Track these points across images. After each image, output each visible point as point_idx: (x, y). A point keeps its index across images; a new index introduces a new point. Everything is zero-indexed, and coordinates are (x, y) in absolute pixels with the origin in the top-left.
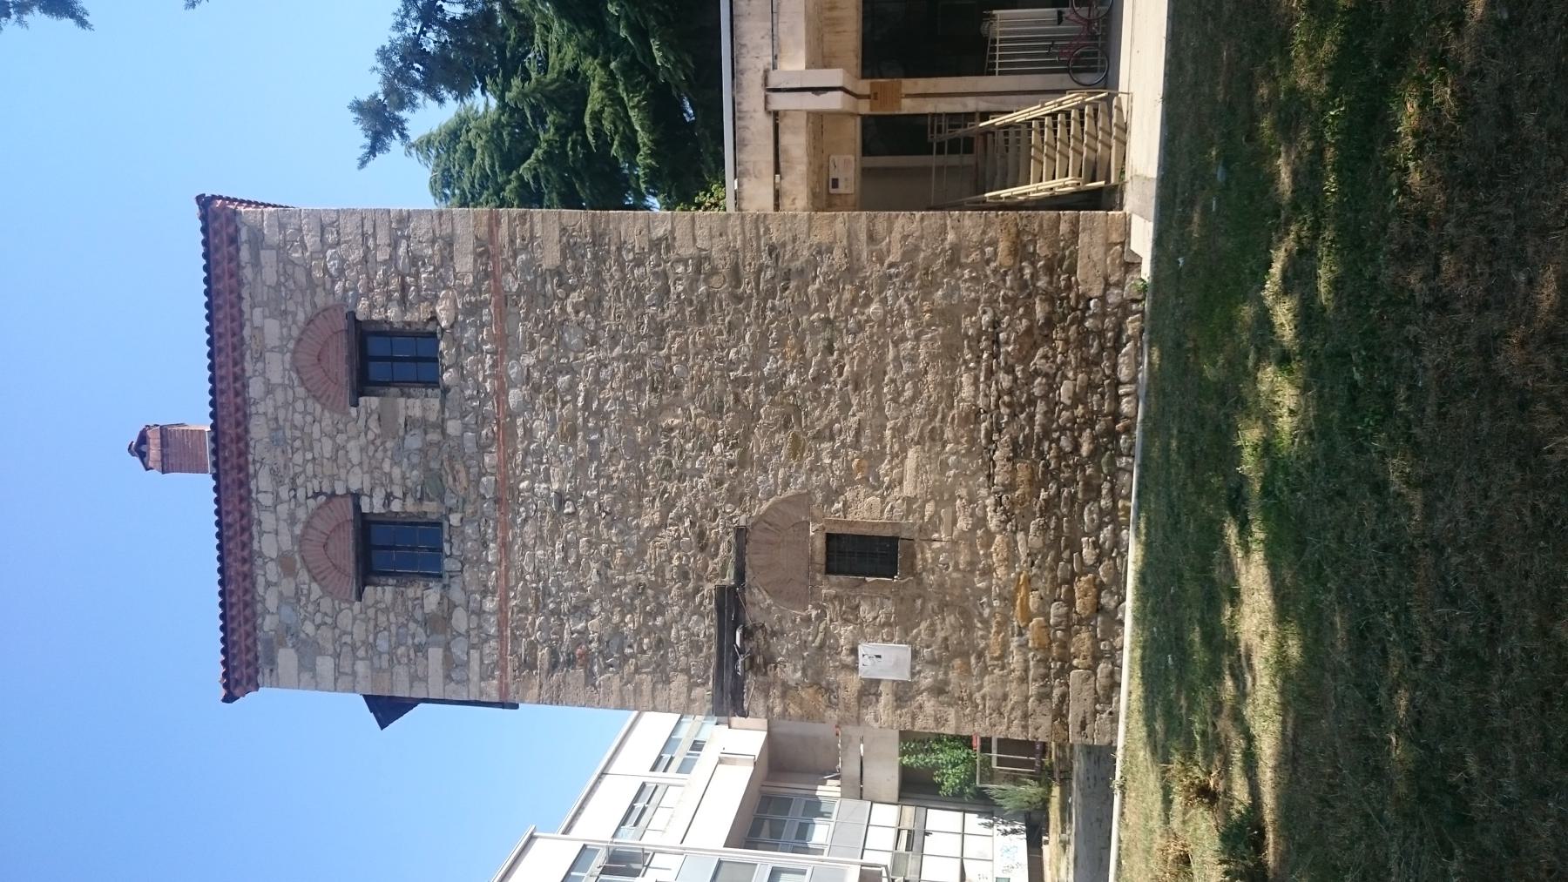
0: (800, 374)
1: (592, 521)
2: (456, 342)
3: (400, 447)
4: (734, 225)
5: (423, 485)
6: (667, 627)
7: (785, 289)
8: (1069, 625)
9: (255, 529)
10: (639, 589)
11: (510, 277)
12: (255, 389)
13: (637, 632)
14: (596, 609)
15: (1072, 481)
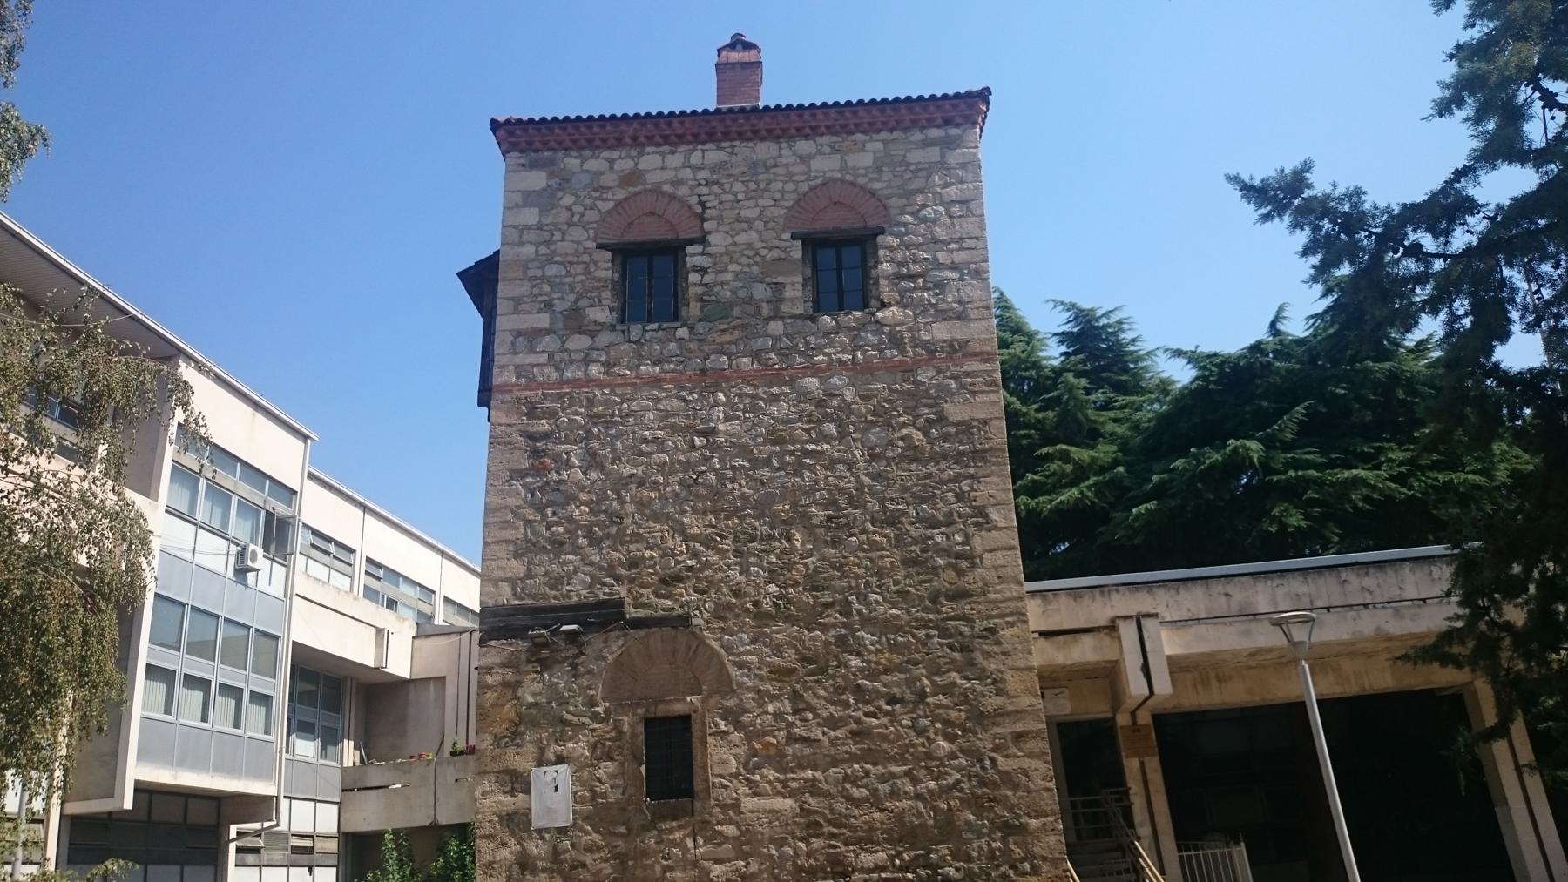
0: (861, 670)
1: (687, 466)
2: (862, 326)
3: (754, 280)
4: (1014, 590)
5: (717, 302)
7: (952, 648)
11: (931, 373)
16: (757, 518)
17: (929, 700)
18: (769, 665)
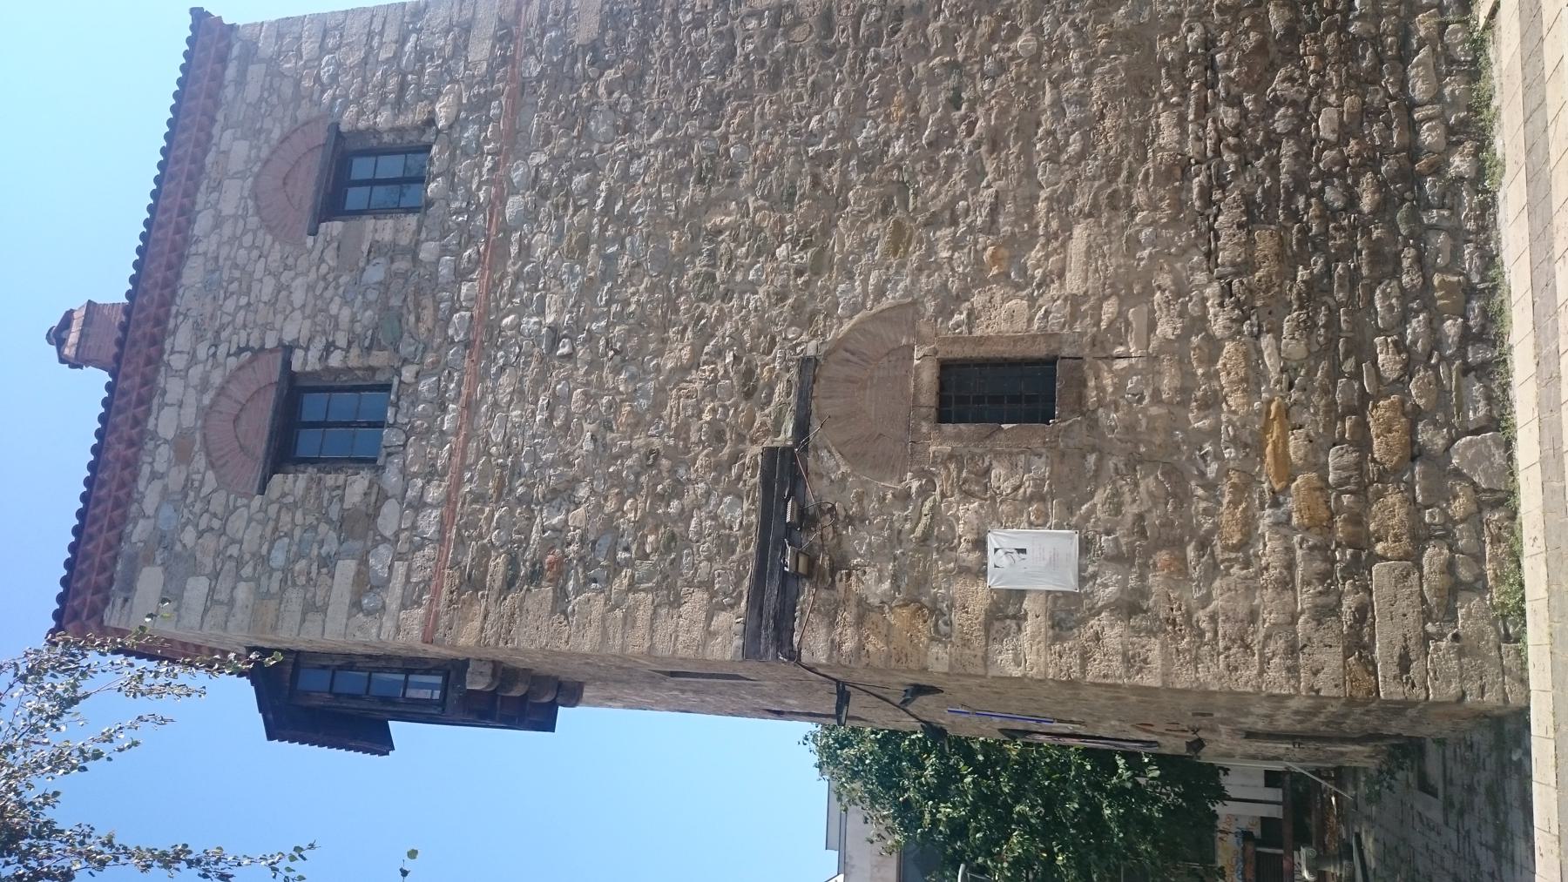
0: (909, 140)
1: (594, 364)
2: (453, 145)
5: (376, 329)
6: (684, 516)
7: (894, 32)
8: (1363, 484)
9: (155, 401)
10: (652, 457)
11: (532, 60)
13: (639, 525)
14: (583, 492)
15: (1349, 250)
16: (682, 270)
17: (960, 57)
18: (885, 255)
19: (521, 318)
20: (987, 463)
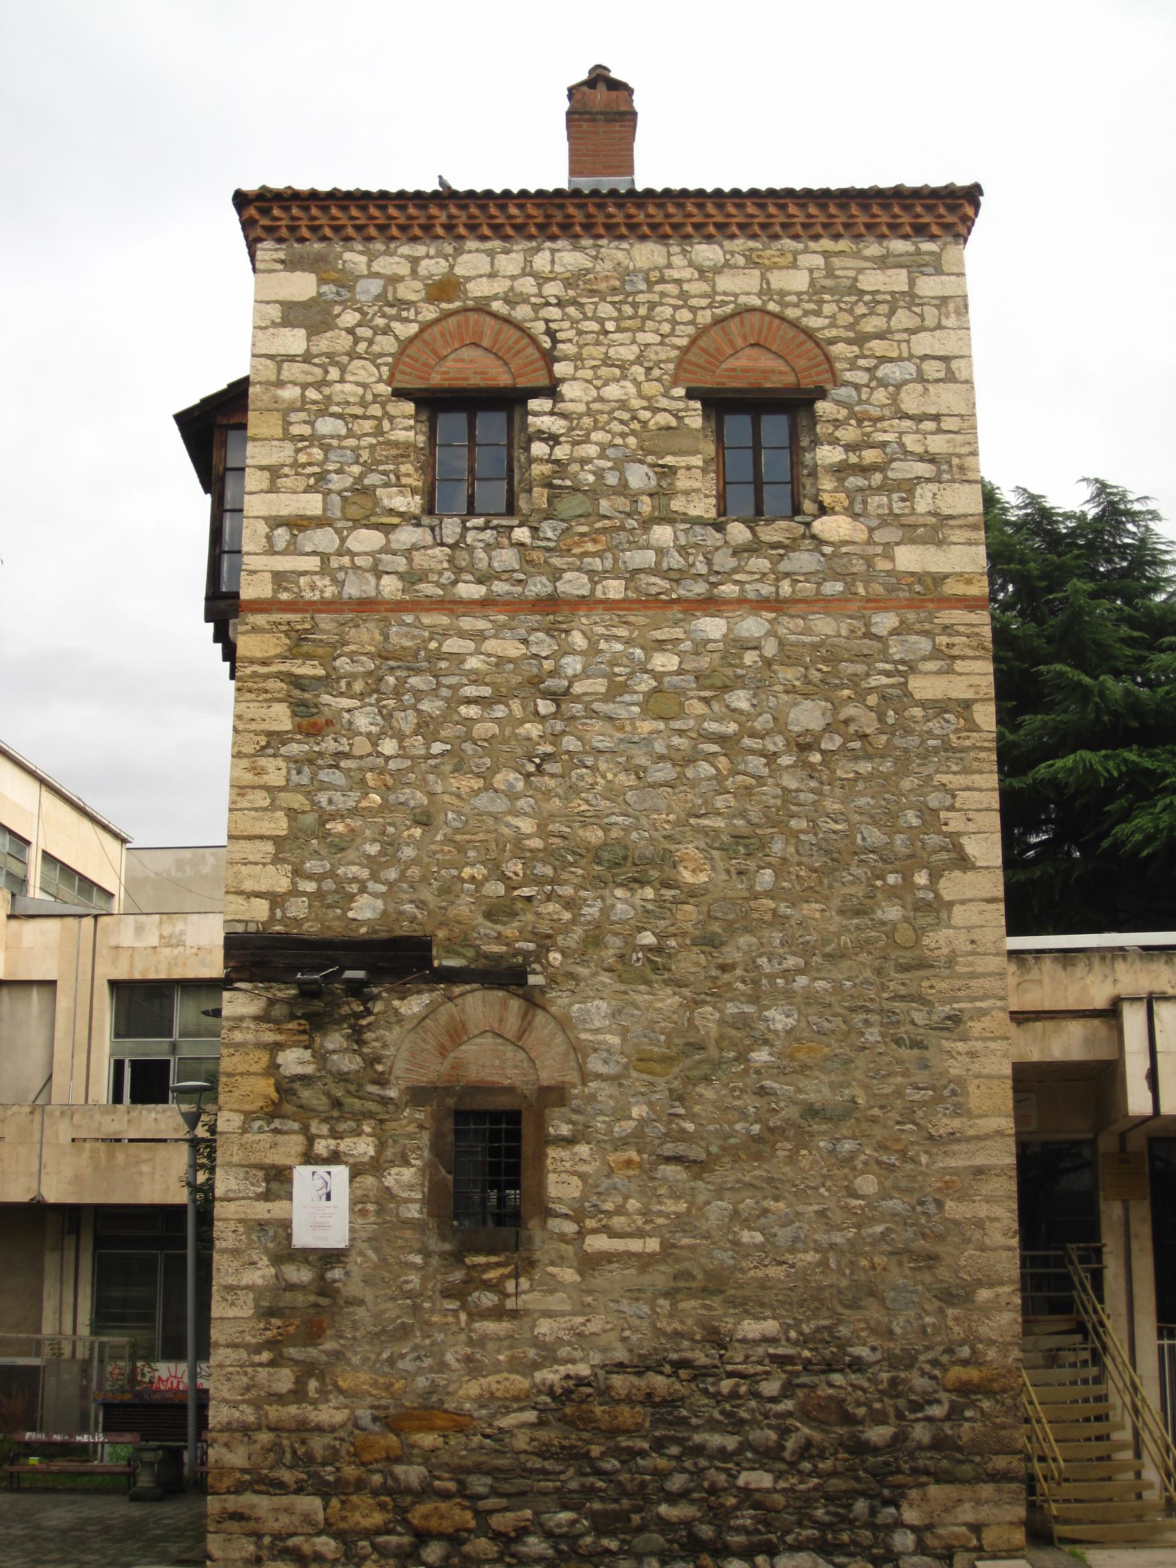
9: (497, 244)
12: (707, 253)
19: (582, 653)
20: (413, 1162)
